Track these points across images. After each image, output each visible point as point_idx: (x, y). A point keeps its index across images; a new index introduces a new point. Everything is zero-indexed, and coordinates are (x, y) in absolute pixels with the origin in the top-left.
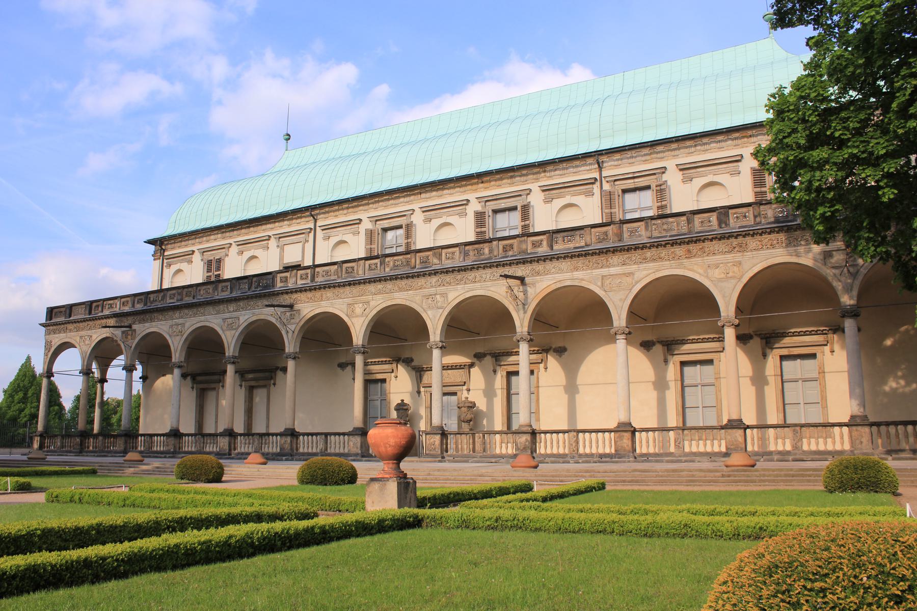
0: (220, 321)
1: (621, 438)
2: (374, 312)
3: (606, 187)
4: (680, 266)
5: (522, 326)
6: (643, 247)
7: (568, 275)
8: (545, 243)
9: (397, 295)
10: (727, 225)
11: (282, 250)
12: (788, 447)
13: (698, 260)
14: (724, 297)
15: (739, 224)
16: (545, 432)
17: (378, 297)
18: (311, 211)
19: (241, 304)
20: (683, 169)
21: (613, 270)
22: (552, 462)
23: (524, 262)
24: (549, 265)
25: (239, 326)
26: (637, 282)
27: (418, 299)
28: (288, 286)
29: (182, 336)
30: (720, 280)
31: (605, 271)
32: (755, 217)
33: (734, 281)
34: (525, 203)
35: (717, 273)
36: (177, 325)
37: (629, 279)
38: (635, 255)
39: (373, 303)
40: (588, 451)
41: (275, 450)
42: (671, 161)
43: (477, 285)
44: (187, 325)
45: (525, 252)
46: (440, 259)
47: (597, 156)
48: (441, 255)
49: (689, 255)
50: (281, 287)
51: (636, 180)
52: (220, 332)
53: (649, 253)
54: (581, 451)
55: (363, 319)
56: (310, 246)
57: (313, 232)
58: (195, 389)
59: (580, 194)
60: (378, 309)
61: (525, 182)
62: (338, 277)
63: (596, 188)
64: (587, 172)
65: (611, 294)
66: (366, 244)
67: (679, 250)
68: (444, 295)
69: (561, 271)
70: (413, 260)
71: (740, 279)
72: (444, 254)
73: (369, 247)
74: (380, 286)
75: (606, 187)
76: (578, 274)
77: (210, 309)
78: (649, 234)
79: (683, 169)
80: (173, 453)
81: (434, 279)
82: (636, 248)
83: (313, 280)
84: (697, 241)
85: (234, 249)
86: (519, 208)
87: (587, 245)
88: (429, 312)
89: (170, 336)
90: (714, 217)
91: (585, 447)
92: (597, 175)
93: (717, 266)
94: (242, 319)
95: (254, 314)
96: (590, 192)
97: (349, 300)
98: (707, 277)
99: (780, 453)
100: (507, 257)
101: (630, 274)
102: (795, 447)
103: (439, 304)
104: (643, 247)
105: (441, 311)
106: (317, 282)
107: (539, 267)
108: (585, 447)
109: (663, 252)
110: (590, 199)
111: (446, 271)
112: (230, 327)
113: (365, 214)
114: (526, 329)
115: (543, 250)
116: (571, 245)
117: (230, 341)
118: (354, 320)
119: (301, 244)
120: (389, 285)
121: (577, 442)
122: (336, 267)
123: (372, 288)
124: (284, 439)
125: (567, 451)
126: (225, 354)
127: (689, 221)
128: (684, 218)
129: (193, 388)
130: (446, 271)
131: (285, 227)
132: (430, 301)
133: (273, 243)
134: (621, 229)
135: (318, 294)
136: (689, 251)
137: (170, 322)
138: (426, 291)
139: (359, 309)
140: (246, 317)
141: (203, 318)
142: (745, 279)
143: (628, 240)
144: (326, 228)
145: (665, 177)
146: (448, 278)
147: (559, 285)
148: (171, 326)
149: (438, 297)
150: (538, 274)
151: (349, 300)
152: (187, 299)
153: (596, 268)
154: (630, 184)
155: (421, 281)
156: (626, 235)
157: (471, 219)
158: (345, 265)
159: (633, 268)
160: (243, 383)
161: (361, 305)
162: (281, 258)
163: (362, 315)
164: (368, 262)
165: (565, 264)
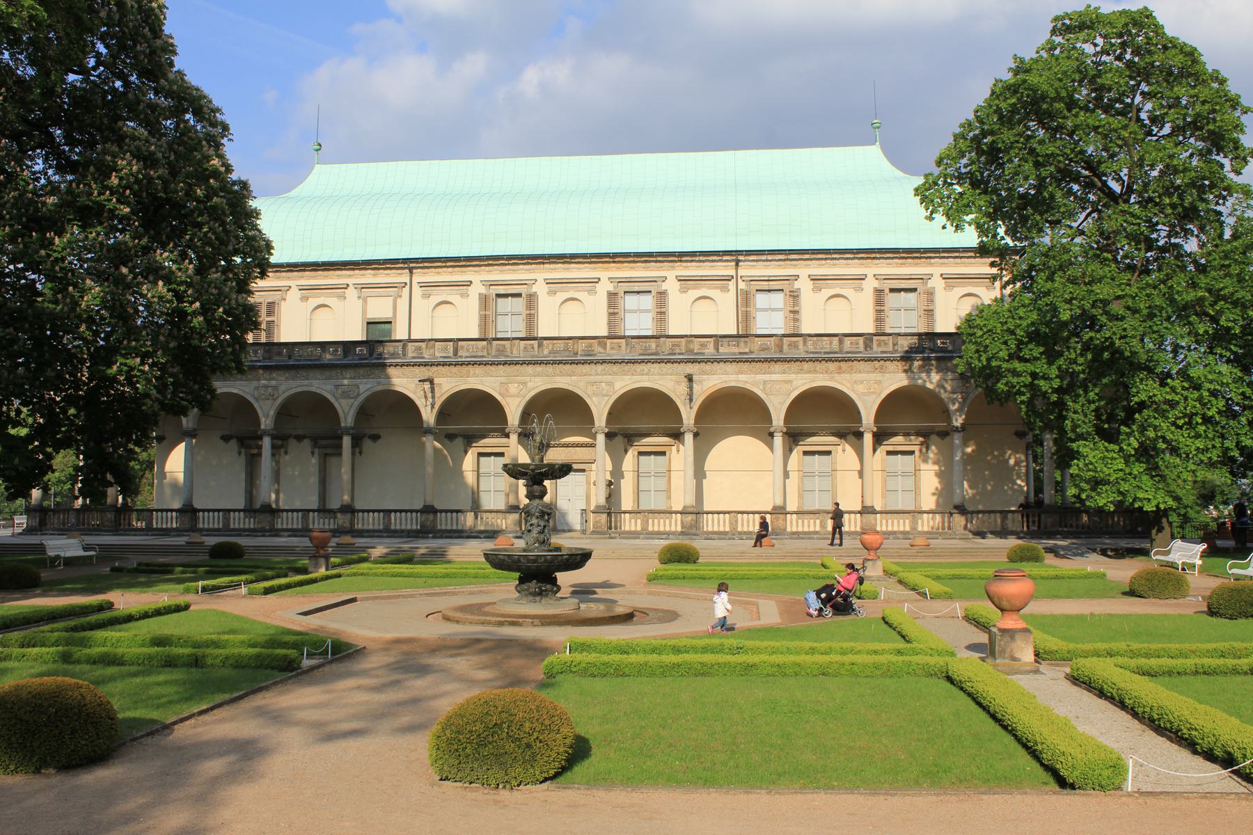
0: (329, 387)
1: (777, 519)
2: (533, 393)
3: (742, 285)
4: (832, 379)
5: (688, 419)
6: (803, 360)
7: (733, 377)
8: (712, 345)
9: (558, 379)
10: (871, 349)
11: (365, 301)
12: (908, 528)
13: (847, 376)
14: (866, 408)
15: (881, 350)
16: (707, 513)
17: (538, 379)
18: (409, 264)
19: (361, 371)
20: (814, 279)
21: (774, 377)
22: (719, 539)
23: (694, 361)
24: (716, 366)
25: (358, 395)
26: (794, 389)
27: (582, 384)
28: (423, 358)
29: (275, 400)
30: (864, 394)
31: (767, 377)
32: (894, 345)
33: (874, 396)
34: (660, 290)
35: (861, 388)
36: (266, 387)
37: (788, 386)
38: (795, 366)
39: (530, 385)
40: (745, 529)
41: (414, 527)
42: (805, 271)
43: (645, 377)
44: (282, 388)
45: (691, 351)
46: (605, 348)
47: (736, 256)
48: (606, 344)
49: (840, 372)
50: (414, 358)
51: (771, 283)
52: (332, 400)
53: (806, 366)
54: (740, 529)
55: (519, 399)
56: (403, 304)
57: (408, 287)
58: (243, 454)
59: (716, 288)
60: (537, 391)
61: (659, 269)
62: (488, 354)
63: (732, 284)
64: (725, 269)
65: (772, 397)
66: (480, 310)
67: (832, 366)
68: (610, 384)
69: (726, 373)
70: (576, 347)
71: (879, 395)
72: (608, 345)
73: (483, 313)
74: (539, 368)
75: (742, 285)
76: (742, 377)
77: (317, 373)
78: (806, 349)
79: (814, 279)
80: (270, 530)
81: (600, 368)
82: (797, 360)
83: (456, 353)
84: (849, 360)
85: (294, 295)
86: (654, 293)
87: (751, 352)
88: (594, 399)
89: (257, 399)
90: (861, 340)
91: (743, 525)
92: (732, 272)
93: (862, 382)
94: (362, 388)
95: (379, 384)
96: (727, 287)
97: (503, 379)
98: (853, 390)
99: (902, 533)
100: (674, 354)
101: (789, 382)
102: (914, 528)
103: (604, 392)
104: (803, 360)
105: (607, 398)
106: (461, 357)
107: (708, 367)
108: (743, 525)
109: (818, 366)
110: (725, 295)
111: (615, 362)
112: (346, 395)
113: (478, 277)
114: (692, 422)
115: (710, 350)
116: (736, 350)
117: (346, 410)
118: (508, 399)
119: (391, 298)
120: (549, 369)
121: (737, 521)
122: (485, 343)
123: (530, 369)
124: (425, 516)
125: (727, 529)
126: (340, 424)
127: (841, 342)
128: (837, 338)
129: (240, 453)
130: (615, 362)
131: (368, 277)
132: (594, 388)
133: (351, 293)
134: (782, 341)
135: (464, 369)
136: (840, 368)
137: (255, 383)
138: (592, 378)
139: (513, 388)
140: (369, 386)
141: (306, 382)
142: (883, 396)
143: (788, 352)
144: (423, 285)
145: (797, 285)
146: (616, 368)
147: (724, 385)
148: (257, 388)
149: (603, 384)
150: (704, 373)
151: (503, 379)
152: (277, 358)
153: (759, 373)
154: (765, 285)
155: (586, 368)
156: (785, 347)
157: (601, 300)
158: (495, 343)
159: (792, 377)
160: (316, 451)
161: (516, 385)
162: (364, 312)
163: (517, 396)
164: (523, 343)
165: (730, 367)
